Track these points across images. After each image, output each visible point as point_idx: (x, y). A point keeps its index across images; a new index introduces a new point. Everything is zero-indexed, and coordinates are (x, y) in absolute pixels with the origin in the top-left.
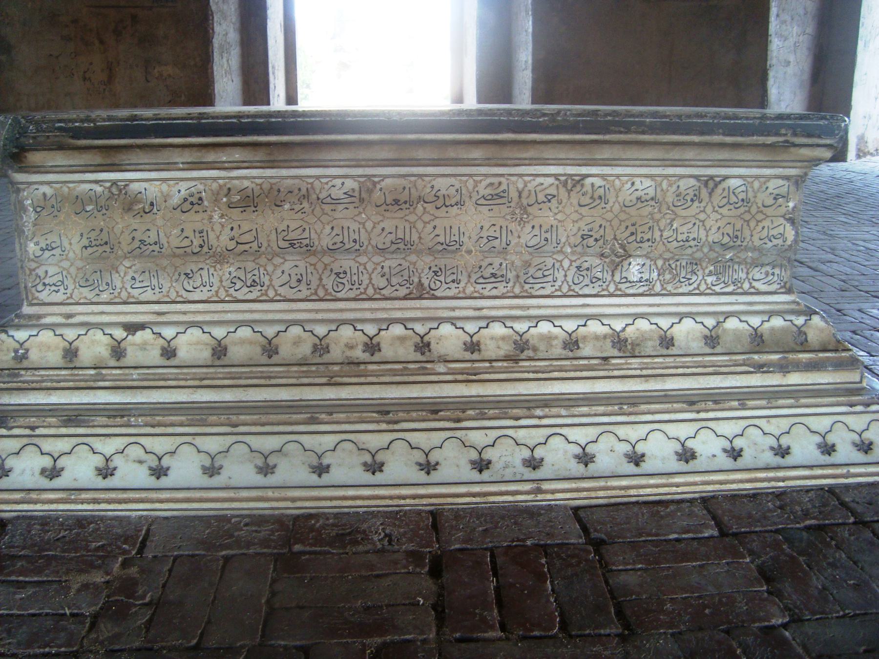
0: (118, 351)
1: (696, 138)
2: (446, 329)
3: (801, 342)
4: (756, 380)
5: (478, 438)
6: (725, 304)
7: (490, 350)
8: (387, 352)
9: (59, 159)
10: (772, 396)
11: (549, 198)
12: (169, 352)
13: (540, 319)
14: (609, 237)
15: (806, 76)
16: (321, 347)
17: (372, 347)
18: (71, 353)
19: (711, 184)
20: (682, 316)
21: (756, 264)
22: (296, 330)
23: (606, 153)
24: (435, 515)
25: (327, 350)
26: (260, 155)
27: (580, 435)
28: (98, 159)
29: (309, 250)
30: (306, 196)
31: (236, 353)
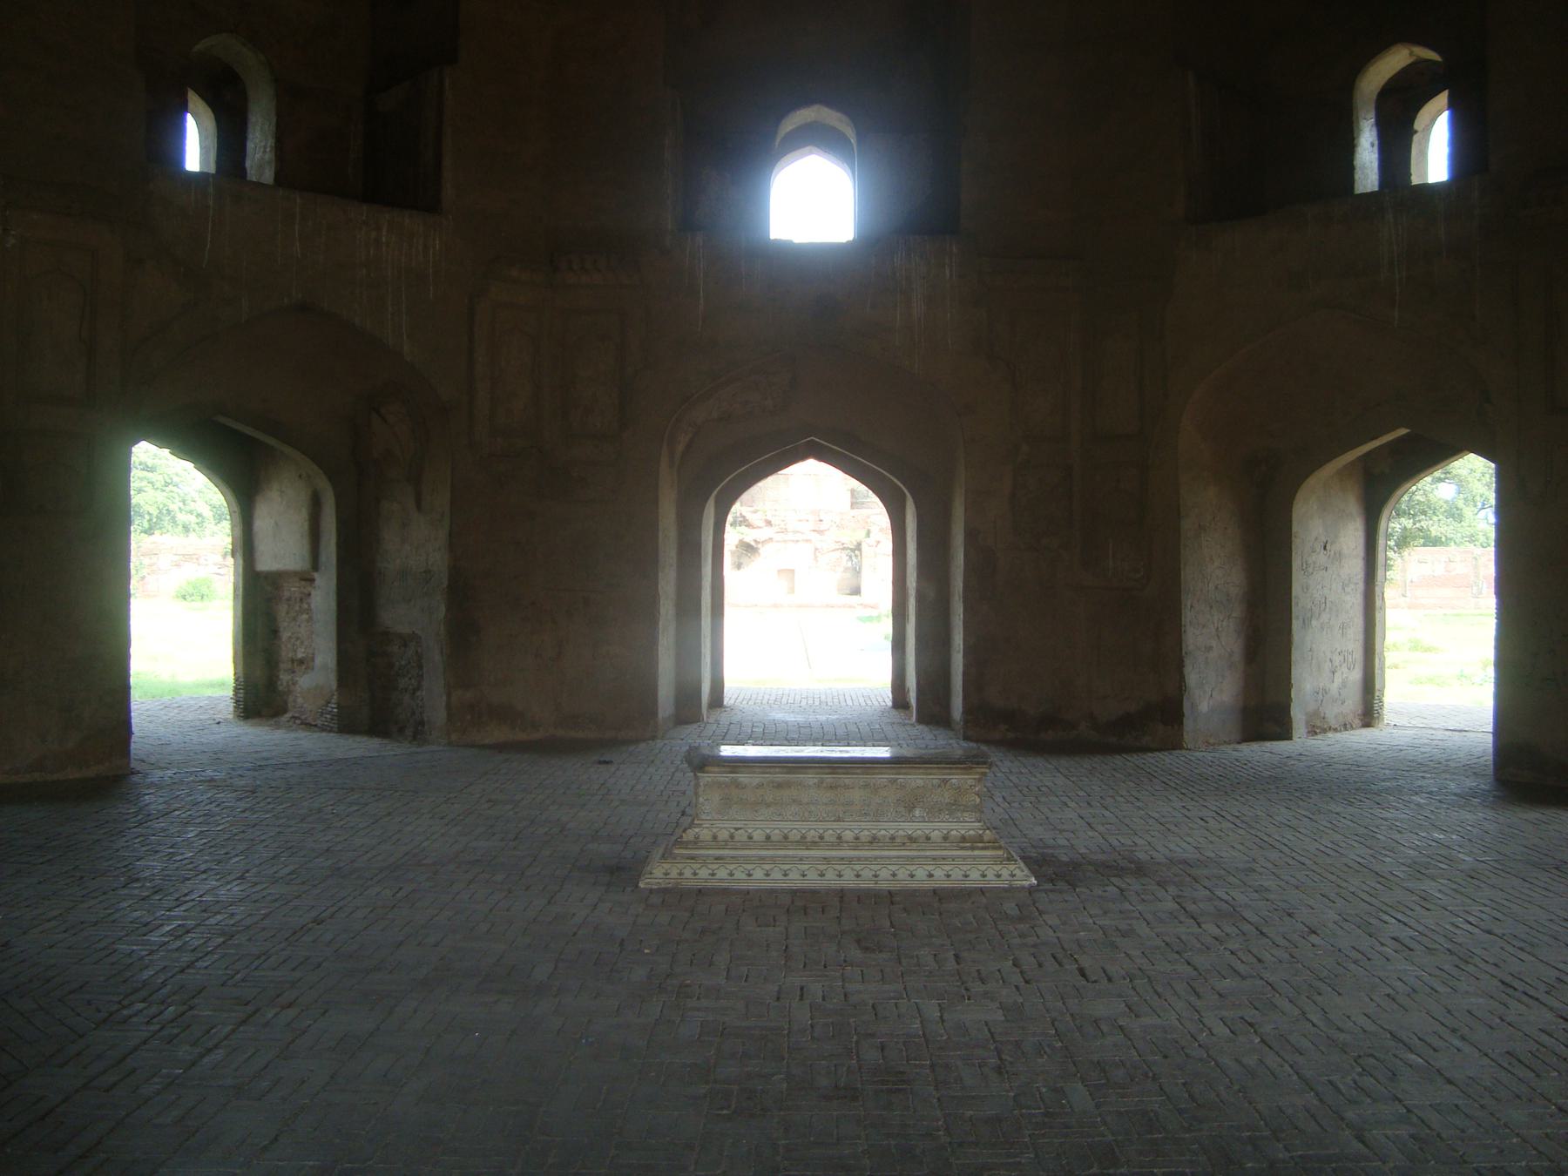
0: (732, 837)
1: (935, 766)
2: (847, 832)
3: (980, 839)
5: (858, 867)
6: (954, 826)
7: (863, 839)
8: (827, 838)
9: (716, 769)
10: (964, 858)
11: (885, 786)
12: (750, 837)
13: (881, 829)
14: (907, 800)
15: (1238, 657)
16: (803, 837)
17: (821, 837)
19: (945, 781)
20: (934, 830)
21: (964, 811)
22: (795, 831)
23: (904, 771)
24: (842, 890)
25: (805, 838)
26: (785, 770)
27: (893, 868)
28: (728, 770)
29: (800, 803)
30: (800, 785)
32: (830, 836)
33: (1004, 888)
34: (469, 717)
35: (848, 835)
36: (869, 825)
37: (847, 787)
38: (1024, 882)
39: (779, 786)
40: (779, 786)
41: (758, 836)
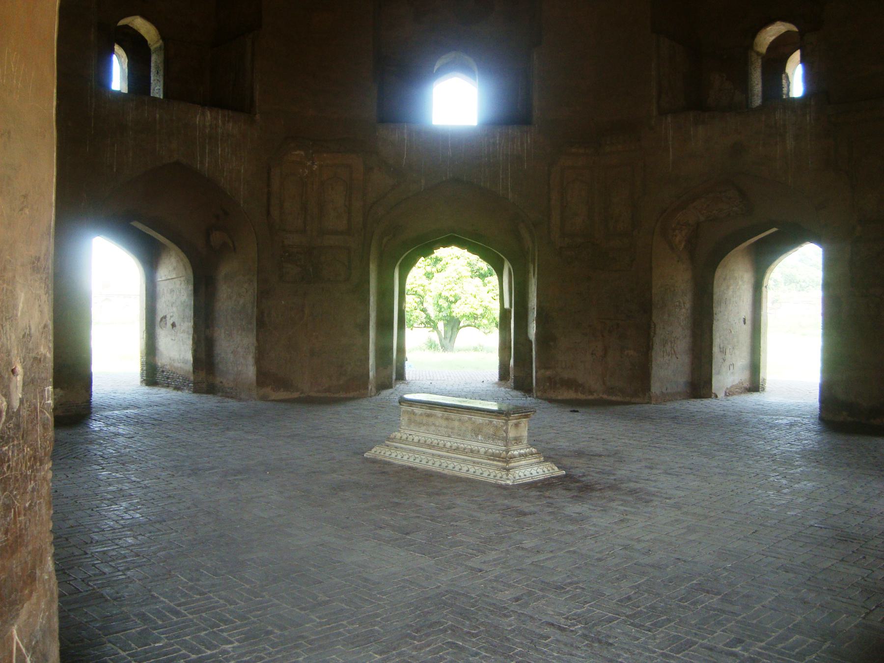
0: (407, 438)
4: (488, 461)
6: (493, 447)
10: (486, 464)
11: (467, 421)
18: (401, 437)
19: (491, 422)
26: (427, 408)
31: (421, 442)
32: (441, 444)
33: (492, 483)
34: (548, 384)
35: (448, 444)
36: (459, 441)
37: (452, 420)
38: (502, 482)
39: (429, 416)
40: (429, 416)
41: (416, 439)
